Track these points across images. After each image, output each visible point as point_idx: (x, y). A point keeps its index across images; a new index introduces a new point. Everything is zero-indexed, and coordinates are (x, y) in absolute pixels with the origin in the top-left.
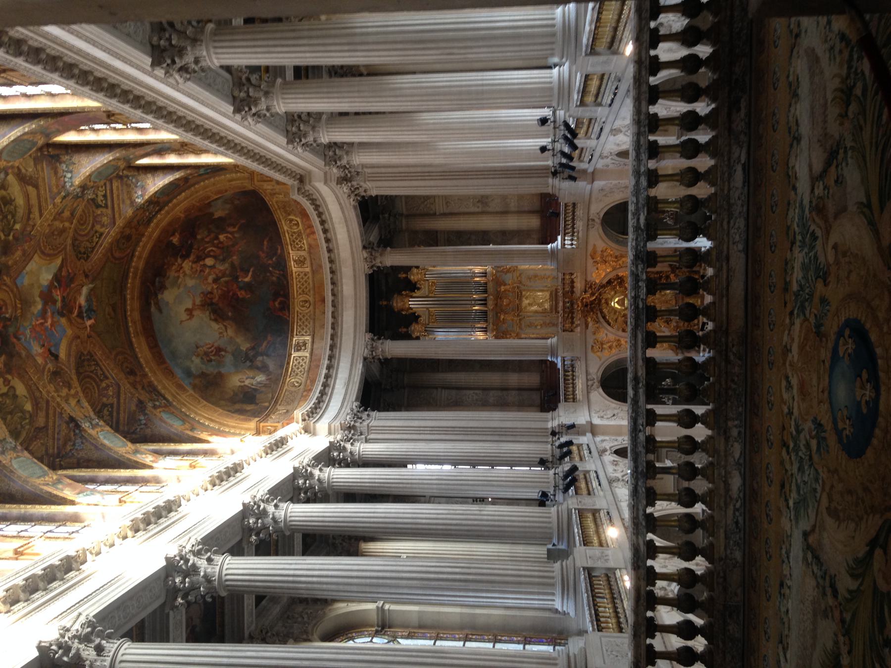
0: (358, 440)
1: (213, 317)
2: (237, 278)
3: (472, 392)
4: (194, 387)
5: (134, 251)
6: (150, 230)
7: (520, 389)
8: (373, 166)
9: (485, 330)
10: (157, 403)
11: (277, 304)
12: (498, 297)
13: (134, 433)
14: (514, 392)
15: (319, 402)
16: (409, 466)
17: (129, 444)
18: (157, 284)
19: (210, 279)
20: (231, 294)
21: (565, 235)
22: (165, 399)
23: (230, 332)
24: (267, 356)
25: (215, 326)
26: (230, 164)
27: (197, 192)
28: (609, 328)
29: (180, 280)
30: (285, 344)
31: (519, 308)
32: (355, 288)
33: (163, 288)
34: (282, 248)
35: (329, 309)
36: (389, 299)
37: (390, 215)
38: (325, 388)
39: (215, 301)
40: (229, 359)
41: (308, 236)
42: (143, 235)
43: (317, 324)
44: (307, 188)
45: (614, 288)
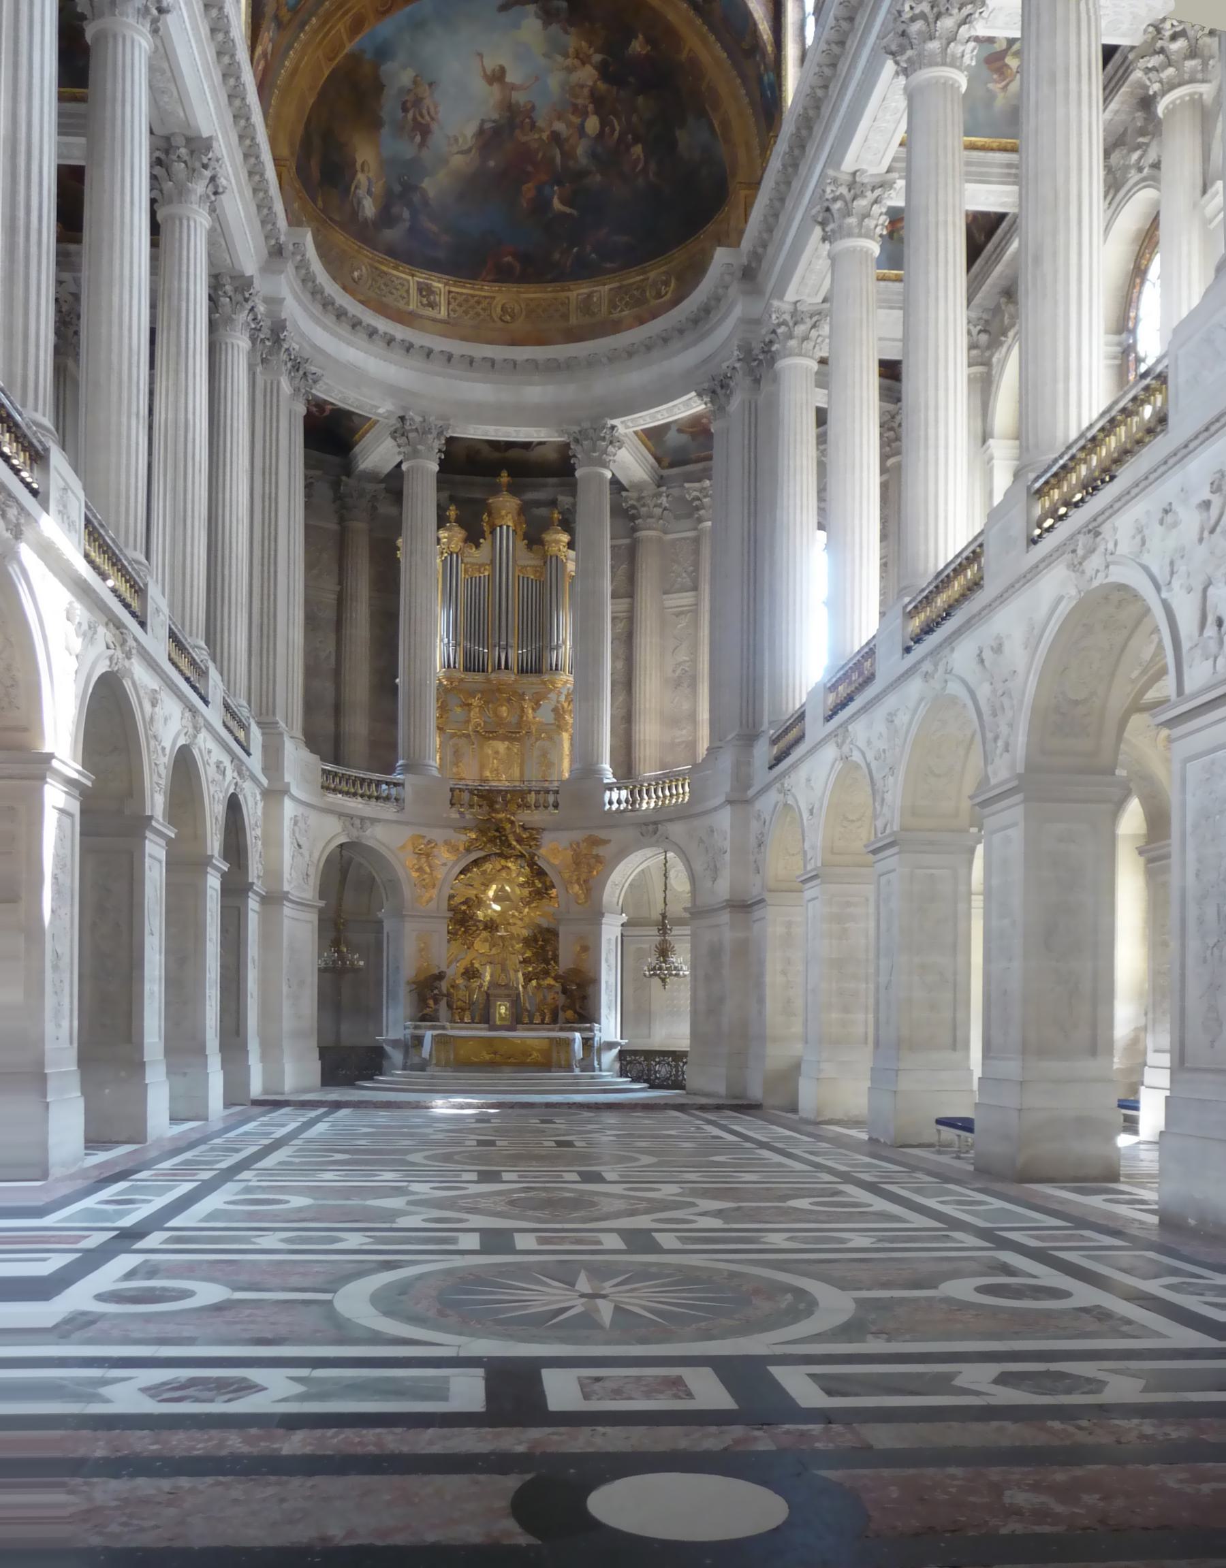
3: (331, 648)
23: (458, 161)
24: (413, 231)
25: (471, 130)
28: (457, 869)
29: (559, 58)
30: (433, 265)
31: (489, 734)
33: (548, 16)
36: (514, 490)
37: (665, 509)
39: (518, 132)
40: (406, 149)
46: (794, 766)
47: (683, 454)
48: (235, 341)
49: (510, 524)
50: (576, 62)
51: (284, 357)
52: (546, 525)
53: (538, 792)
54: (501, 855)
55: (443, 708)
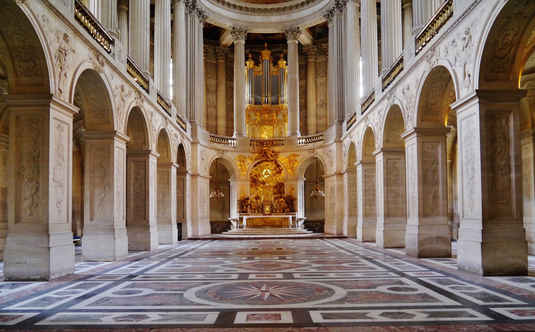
3: (215, 99)
8: (345, 18)
12: (270, 111)
14: (215, 123)
16: (171, 60)
21: (306, 139)
32: (275, 23)
36: (269, 48)
45: (275, 169)
46: (353, 129)
47: (320, 34)
51: (196, 10)
52: (279, 58)
53: (277, 141)
54: (266, 161)
55: (249, 116)
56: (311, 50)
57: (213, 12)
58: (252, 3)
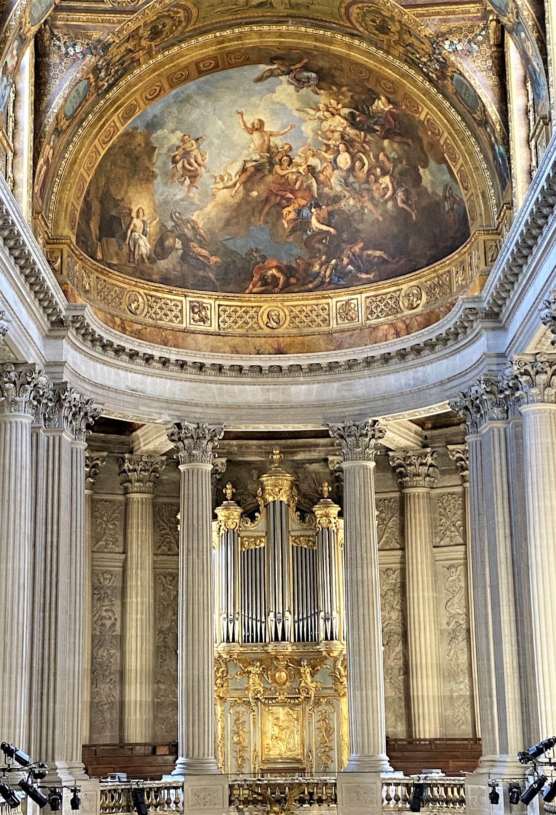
0: (36, 414)
1: (249, 165)
2: (317, 206)
3: (118, 616)
4: (129, 135)
5: (361, 37)
6: (397, 63)
7: (122, 704)
9: (229, 639)
10: (103, 74)
11: (274, 271)
13: (52, 32)
14: (116, 693)
15: (104, 346)
17: (35, 29)
18: (305, 74)
19: (314, 161)
20: (291, 196)
22: (111, 87)
23: (224, 195)
24: (183, 258)
26: (513, 195)
27: (463, 140)
29: (312, 112)
30: (202, 285)
32: (302, 406)
33: (300, 83)
34: (370, 282)
35: (266, 361)
37: (431, 465)
38: (127, 354)
39: (277, 167)
41: (392, 325)
42: (388, 52)
43: (237, 340)
44: (475, 325)
48: (18, 420)
49: (284, 499)
50: (326, 113)
56: (414, 460)
57: (116, 391)
58: (235, 350)
